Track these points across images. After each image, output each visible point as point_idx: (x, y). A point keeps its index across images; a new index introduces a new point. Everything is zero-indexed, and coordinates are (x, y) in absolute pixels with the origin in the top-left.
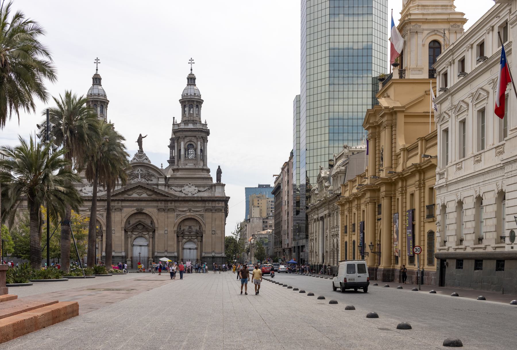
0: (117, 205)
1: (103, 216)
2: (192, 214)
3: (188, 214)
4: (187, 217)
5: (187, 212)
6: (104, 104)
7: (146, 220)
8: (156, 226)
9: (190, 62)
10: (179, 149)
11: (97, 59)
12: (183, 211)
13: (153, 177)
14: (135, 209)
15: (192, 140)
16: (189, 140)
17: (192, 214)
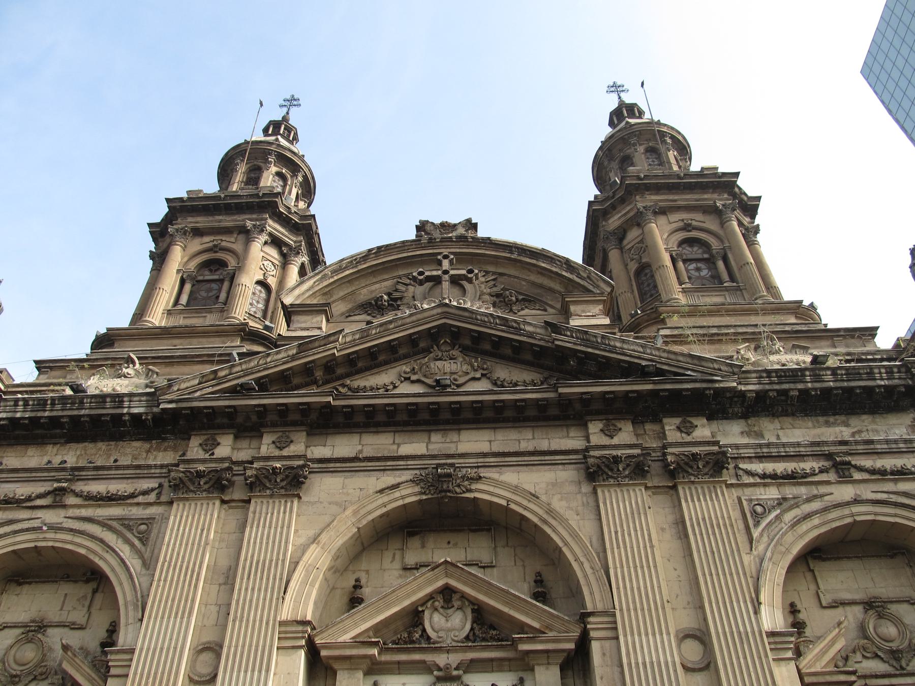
0: (277, 453)
1: (144, 540)
2: (867, 492)
3: (846, 492)
4: (838, 519)
5: (828, 483)
6: (292, 177)
7: (492, 577)
8: (593, 599)
9: (613, 89)
10: (633, 266)
11: (293, 99)
12: (792, 478)
13: (526, 311)
14: (407, 476)
15: (694, 223)
16: (681, 224)
17: (867, 492)
